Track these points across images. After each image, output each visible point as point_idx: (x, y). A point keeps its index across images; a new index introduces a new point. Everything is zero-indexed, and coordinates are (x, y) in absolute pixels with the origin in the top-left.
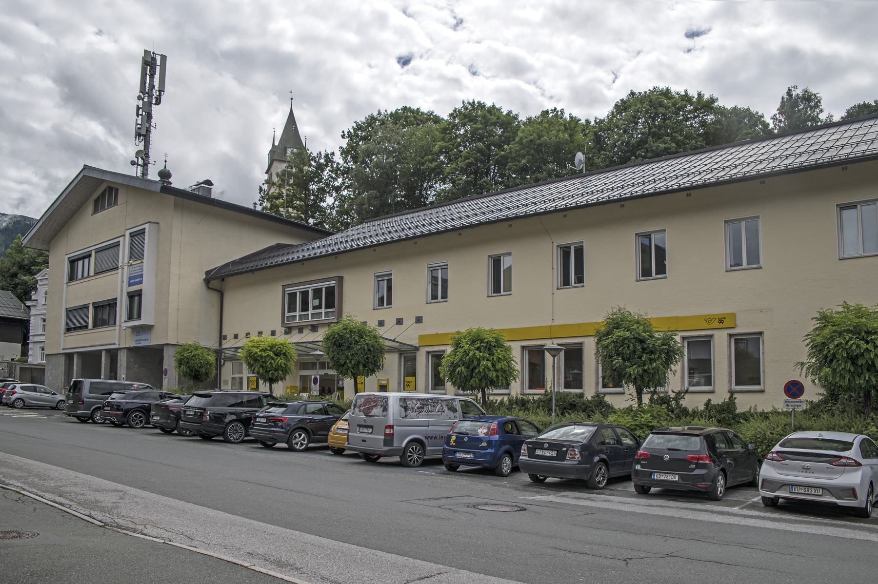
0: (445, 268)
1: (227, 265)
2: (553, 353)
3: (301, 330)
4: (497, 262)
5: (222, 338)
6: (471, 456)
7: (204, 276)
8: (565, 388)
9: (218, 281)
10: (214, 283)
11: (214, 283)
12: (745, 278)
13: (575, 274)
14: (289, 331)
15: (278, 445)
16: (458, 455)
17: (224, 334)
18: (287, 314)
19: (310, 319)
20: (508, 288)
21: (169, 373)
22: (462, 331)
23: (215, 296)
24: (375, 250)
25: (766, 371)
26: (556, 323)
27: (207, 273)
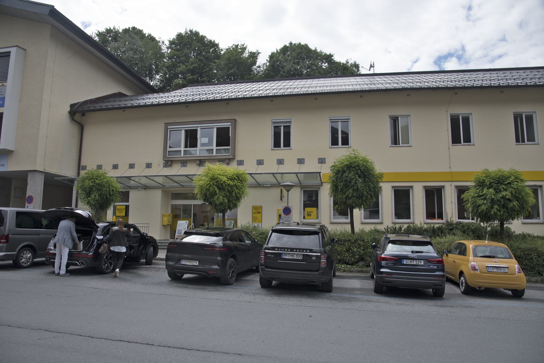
0: (346, 121)
1: (86, 102)
2: (287, 188)
3: (184, 163)
4: (395, 120)
5: (80, 167)
6: (196, 263)
7: (68, 109)
8: (459, 218)
9: (80, 113)
10: (78, 117)
11: (78, 117)
12: (526, 148)
13: (338, 137)
14: (168, 163)
15: (186, 276)
16: (183, 262)
17: (83, 164)
18: (169, 149)
19: (214, 154)
20: (407, 141)
21: (34, 201)
22: (490, 170)
23: (74, 130)
24: (316, 99)
25: (384, 203)
26: (453, 170)
27: (72, 106)
